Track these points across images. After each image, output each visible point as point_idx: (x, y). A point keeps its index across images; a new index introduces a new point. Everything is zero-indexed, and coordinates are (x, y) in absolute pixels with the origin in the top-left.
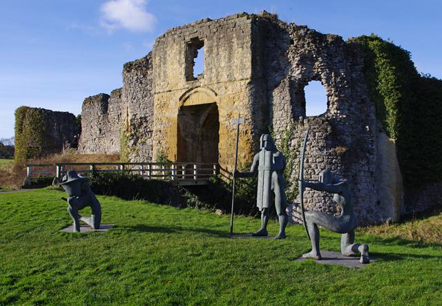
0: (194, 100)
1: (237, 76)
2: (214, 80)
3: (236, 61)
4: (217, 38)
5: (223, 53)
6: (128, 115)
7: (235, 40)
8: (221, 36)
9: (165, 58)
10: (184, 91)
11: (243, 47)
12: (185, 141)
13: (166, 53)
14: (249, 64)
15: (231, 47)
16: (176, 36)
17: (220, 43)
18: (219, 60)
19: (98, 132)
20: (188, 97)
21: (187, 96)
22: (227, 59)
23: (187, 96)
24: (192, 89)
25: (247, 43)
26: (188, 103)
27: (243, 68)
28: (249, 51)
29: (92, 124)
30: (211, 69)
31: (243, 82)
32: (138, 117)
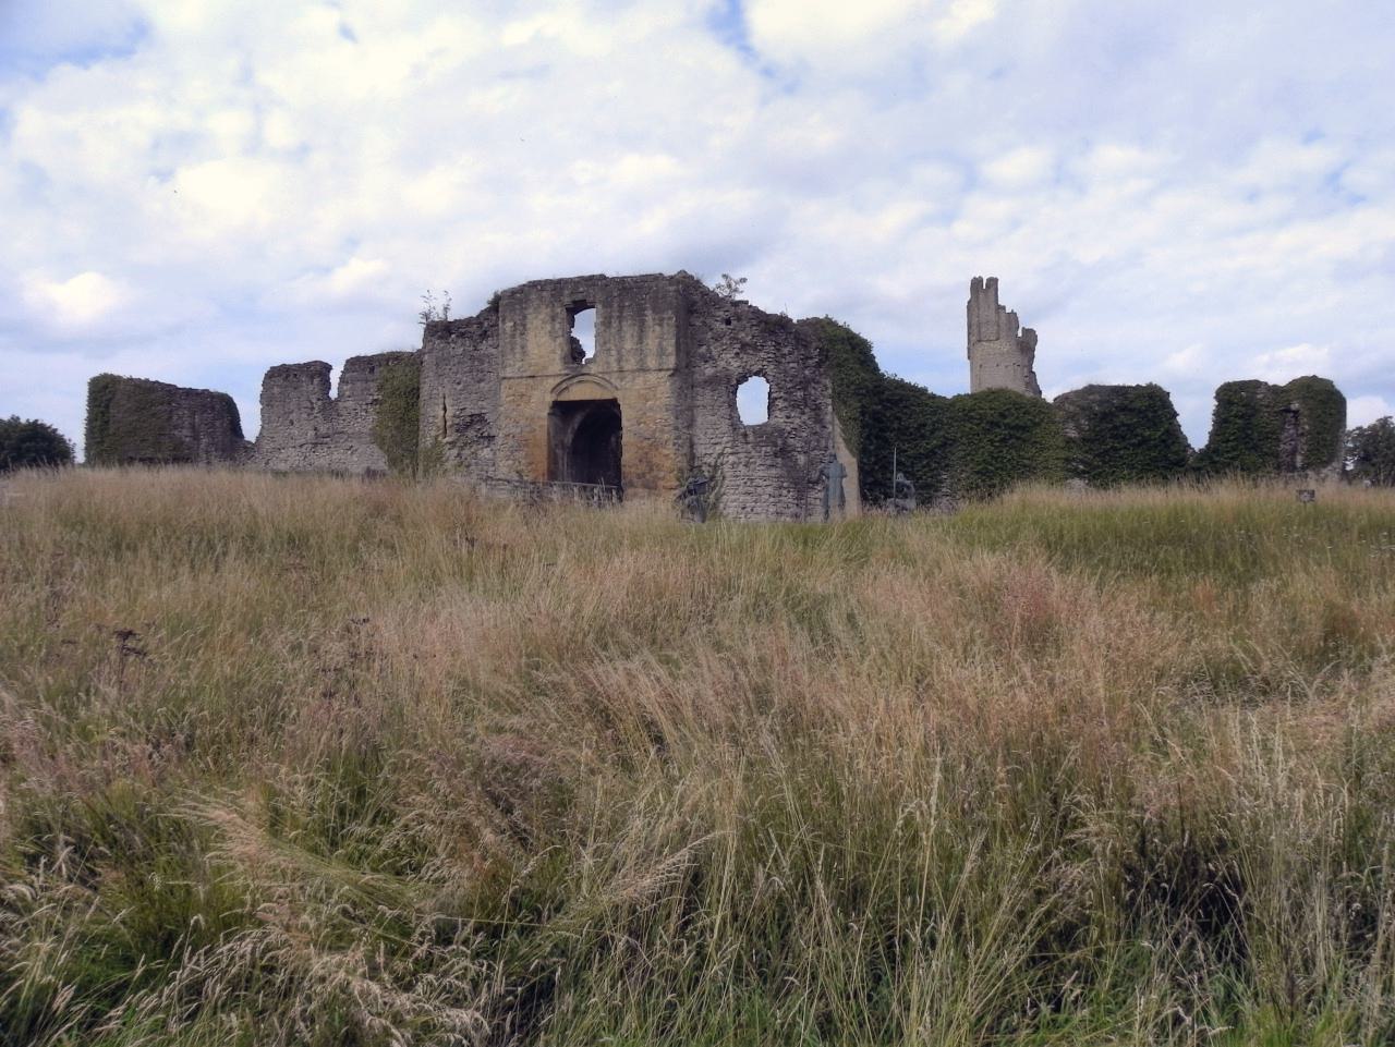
0: (578, 393)
1: (652, 363)
2: (615, 366)
3: (651, 342)
5: (629, 331)
6: (445, 409)
9: (524, 326)
10: (558, 380)
11: (661, 325)
12: (555, 454)
13: (525, 317)
14: (671, 349)
16: (544, 294)
18: (622, 338)
19: (311, 433)
20: (566, 388)
21: (564, 385)
22: (636, 339)
23: (564, 385)
24: (573, 377)
25: (670, 318)
26: (566, 397)
27: (661, 352)
28: (673, 330)
29: (293, 416)
30: (609, 350)
32: (468, 412)
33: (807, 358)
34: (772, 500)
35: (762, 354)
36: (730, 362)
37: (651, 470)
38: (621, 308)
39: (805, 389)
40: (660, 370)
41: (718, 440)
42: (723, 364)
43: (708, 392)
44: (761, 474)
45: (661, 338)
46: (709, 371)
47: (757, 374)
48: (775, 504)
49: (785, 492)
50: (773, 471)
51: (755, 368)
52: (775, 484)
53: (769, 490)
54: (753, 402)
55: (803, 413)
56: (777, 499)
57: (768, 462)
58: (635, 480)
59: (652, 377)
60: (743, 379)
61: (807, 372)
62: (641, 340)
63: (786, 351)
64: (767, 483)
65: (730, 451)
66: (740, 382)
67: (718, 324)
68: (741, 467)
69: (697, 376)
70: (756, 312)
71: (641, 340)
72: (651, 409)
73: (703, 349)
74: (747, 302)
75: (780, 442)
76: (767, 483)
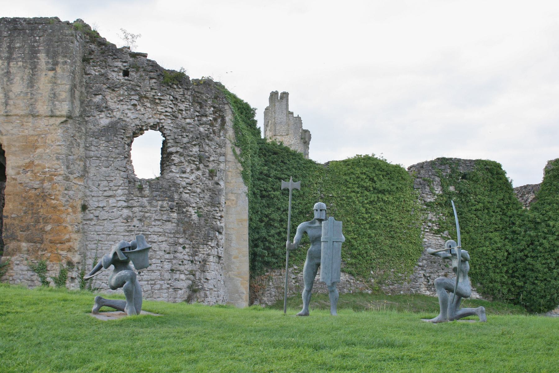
1: (42, 108)
4: (9, 47)
7: (42, 56)
8: (18, 45)
15: (34, 67)
17: (14, 56)
22: (26, 82)
31: (52, 121)
33: (202, 116)
34: (167, 256)
35: (159, 108)
36: (125, 112)
37: (37, 222)
38: (11, 50)
39: (200, 145)
40: (52, 116)
41: (111, 193)
42: (118, 114)
43: (103, 143)
44: (156, 229)
45: (54, 82)
46: (104, 121)
47: (153, 127)
48: (170, 261)
49: (180, 248)
50: (169, 226)
51: (152, 122)
52: (171, 240)
53: (164, 246)
54: (146, 157)
55: (198, 169)
56: (172, 256)
58: (19, 233)
59: (42, 123)
60: (140, 131)
61: (202, 129)
62: (31, 83)
63: (182, 107)
64: (161, 239)
65: (125, 204)
66: (135, 135)
67: (114, 74)
68: (136, 222)
69: (90, 126)
70: (154, 65)
71: (31, 83)
72: (41, 157)
73: (98, 99)
74: (145, 55)
75: (176, 197)
76: (161, 239)
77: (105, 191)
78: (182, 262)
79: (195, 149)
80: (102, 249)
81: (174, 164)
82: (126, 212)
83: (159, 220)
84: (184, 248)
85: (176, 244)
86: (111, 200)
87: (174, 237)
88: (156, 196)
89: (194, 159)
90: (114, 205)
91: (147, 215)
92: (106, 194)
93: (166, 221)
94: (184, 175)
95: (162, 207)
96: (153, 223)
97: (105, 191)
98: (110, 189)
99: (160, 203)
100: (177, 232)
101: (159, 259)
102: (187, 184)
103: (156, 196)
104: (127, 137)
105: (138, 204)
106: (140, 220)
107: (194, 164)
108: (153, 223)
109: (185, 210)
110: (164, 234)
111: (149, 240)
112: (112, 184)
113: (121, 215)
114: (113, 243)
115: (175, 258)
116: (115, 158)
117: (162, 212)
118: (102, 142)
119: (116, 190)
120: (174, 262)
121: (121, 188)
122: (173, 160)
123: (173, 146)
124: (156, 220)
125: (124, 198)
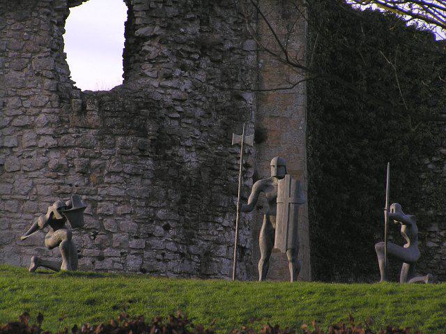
41: (26, 120)
44: (113, 191)
48: (139, 253)
49: (159, 229)
50: (138, 186)
52: (140, 213)
57: (129, 168)
65: (51, 142)
75: (151, 127)
77: (16, 116)
78: (163, 254)
79: (193, 29)
80: (10, 228)
81: (150, 61)
82: (55, 158)
83: (117, 173)
84: (167, 228)
85: (152, 219)
86: (28, 135)
87: (147, 206)
88: (112, 127)
89: (189, 49)
90: (33, 143)
91: (94, 163)
92: (16, 122)
93: (131, 175)
94: (169, 83)
95: (123, 147)
96: (106, 180)
97: (16, 116)
98: (24, 114)
99: (119, 139)
100: (152, 197)
101: (117, 248)
102: (175, 99)
103: (112, 127)
104: (57, 10)
105: (79, 141)
106: (83, 173)
107: (189, 58)
108: (106, 180)
109: (169, 152)
110: (125, 200)
111: (99, 211)
112: (27, 104)
113: (46, 164)
114: (30, 216)
115: (148, 247)
116: (34, 52)
117: (124, 158)
118: (9, 22)
119: (37, 115)
120: (147, 254)
121: (44, 110)
122: (147, 52)
123: (146, 25)
124: (110, 174)
125: (50, 131)
